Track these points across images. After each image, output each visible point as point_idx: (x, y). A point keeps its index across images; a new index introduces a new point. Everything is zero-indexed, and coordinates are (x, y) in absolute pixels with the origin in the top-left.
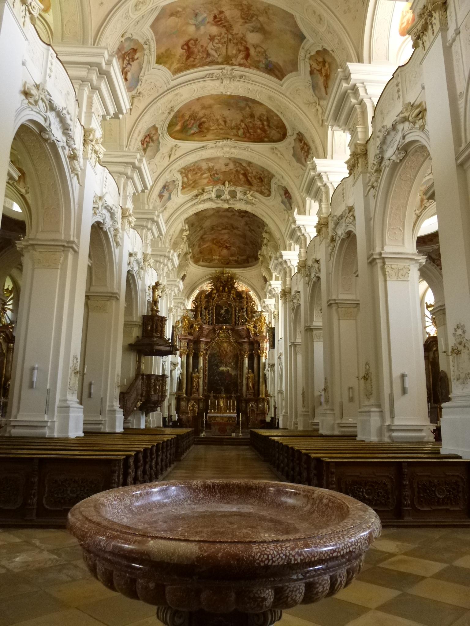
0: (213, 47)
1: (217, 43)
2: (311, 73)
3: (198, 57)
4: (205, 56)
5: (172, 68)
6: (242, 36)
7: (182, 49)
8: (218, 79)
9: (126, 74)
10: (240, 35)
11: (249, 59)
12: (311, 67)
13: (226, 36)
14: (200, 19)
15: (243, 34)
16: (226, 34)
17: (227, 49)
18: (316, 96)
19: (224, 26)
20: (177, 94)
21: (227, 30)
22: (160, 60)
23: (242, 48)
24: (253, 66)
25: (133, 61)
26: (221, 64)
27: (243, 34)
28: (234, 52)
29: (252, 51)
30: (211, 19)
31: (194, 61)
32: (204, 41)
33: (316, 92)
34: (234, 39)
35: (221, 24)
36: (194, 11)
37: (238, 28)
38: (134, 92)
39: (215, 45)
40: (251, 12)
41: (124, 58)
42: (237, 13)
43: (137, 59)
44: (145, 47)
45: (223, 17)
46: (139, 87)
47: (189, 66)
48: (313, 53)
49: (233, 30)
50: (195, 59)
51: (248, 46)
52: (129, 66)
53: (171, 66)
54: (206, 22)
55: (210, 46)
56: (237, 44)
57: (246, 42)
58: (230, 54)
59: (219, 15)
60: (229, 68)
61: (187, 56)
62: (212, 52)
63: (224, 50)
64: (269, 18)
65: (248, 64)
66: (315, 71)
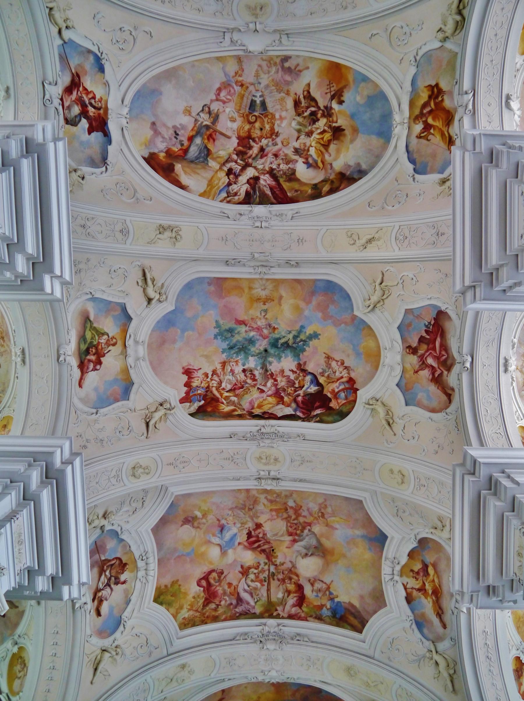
0: (246, 587)
1: (252, 581)
2: (409, 599)
3: (223, 603)
4: (234, 602)
5: (180, 617)
6: (290, 565)
7: (199, 585)
8: (255, 642)
9: (101, 601)
10: (289, 565)
11: (305, 605)
12: (405, 589)
13: (266, 567)
14: (228, 535)
15: (291, 562)
16: (266, 564)
17: (268, 590)
18: (428, 640)
19: (264, 551)
20: (183, 667)
21: (268, 558)
22: (161, 597)
23: (291, 587)
24: (311, 616)
25: (116, 583)
26: (261, 616)
27: (291, 562)
28: (280, 595)
29: (308, 591)
30: (242, 537)
31: (215, 610)
32: (233, 576)
33: (425, 631)
34: (279, 573)
35: (259, 546)
36: (218, 520)
37: (285, 554)
38: (107, 643)
39: (250, 583)
40: (301, 520)
41: (102, 571)
42: (281, 526)
43: (124, 582)
44: (141, 564)
45: (261, 535)
46: (117, 634)
47: (208, 617)
48: (404, 560)
49: (276, 557)
50: (218, 605)
51: (302, 582)
52: (108, 590)
53: (177, 613)
54: (236, 544)
55: (242, 586)
56: (283, 581)
57: (297, 576)
58: (274, 599)
59: (254, 530)
60: (272, 622)
61: (206, 599)
62: (245, 596)
63: (263, 592)
64: (327, 525)
65: (303, 615)
66: (415, 593)
